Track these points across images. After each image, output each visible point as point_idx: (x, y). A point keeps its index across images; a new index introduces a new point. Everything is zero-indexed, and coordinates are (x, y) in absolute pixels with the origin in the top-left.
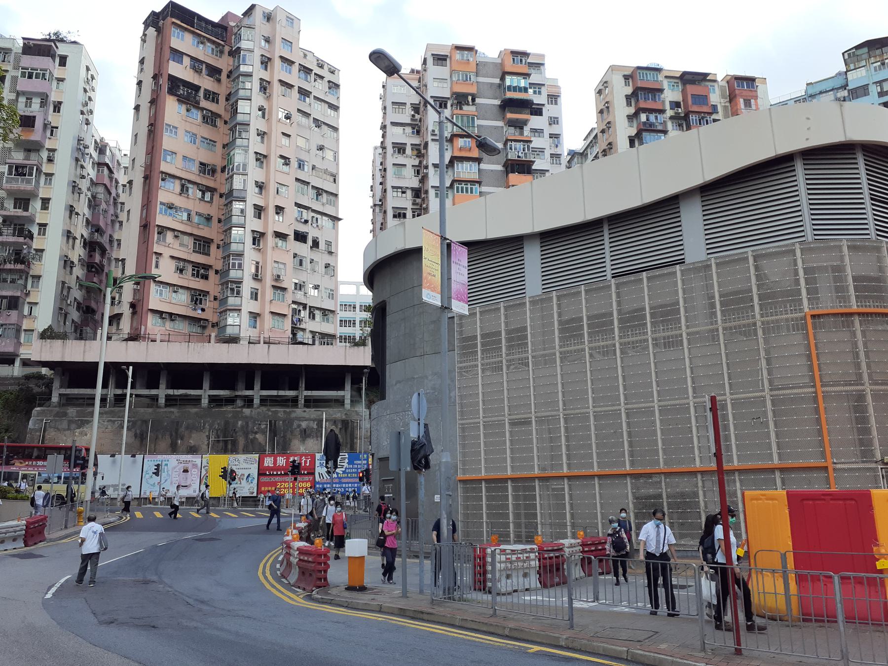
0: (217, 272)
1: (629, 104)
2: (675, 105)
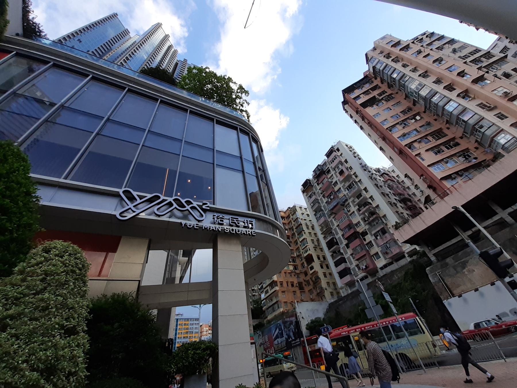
0: (461, 138)
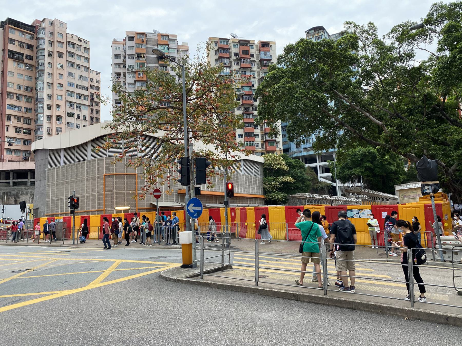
1: (216, 54)
2: (236, 54)
